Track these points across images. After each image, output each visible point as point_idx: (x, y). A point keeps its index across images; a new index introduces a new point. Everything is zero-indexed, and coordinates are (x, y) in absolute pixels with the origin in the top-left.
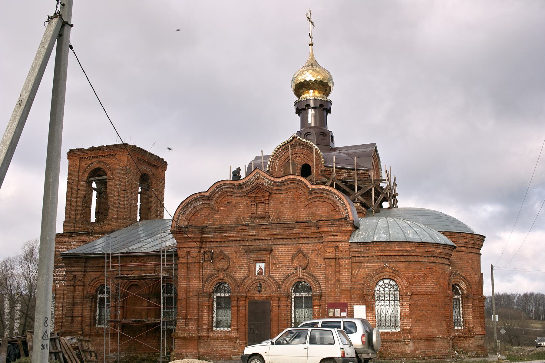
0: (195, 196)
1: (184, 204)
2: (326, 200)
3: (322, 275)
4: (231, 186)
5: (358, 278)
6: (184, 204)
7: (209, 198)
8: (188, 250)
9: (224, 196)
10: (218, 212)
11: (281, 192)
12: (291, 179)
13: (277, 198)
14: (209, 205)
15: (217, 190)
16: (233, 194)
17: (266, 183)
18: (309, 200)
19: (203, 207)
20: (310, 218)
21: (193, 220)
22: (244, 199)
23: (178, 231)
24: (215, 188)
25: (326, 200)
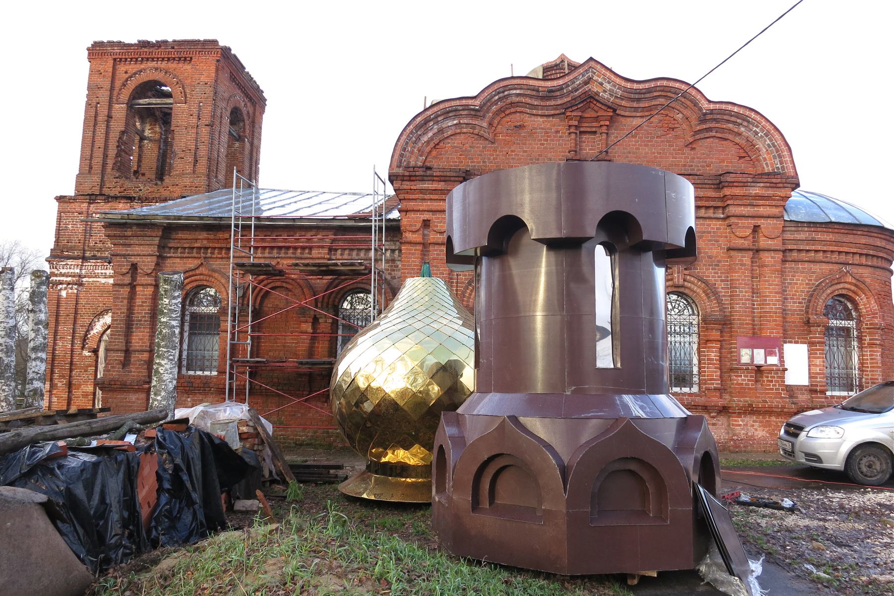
0: (447, 105)
1: (419, 119)
2: (730, 137)
3: (722, 281)
4: (529, 92)
5: (792, 291)
6: (419, 119)
7: (476, 113)
8: (426, 216)
9: (508, 112)
10: (493, 143)
11: (634, 114)
12: (662, 88)
13: (625, 125)
14: (473, 126)
15: (497, 98)
16: (528, 111)
17: (605, 91)
18: (697, 132)
19: (458, 131)
20: (694, 170)
21: (435, 157)
22: (552, 121)
23: (407, 174)
24: (494, 93)
25: (730, 137)
